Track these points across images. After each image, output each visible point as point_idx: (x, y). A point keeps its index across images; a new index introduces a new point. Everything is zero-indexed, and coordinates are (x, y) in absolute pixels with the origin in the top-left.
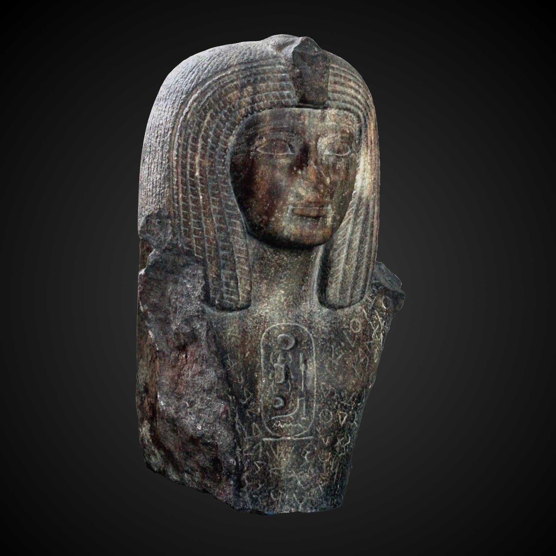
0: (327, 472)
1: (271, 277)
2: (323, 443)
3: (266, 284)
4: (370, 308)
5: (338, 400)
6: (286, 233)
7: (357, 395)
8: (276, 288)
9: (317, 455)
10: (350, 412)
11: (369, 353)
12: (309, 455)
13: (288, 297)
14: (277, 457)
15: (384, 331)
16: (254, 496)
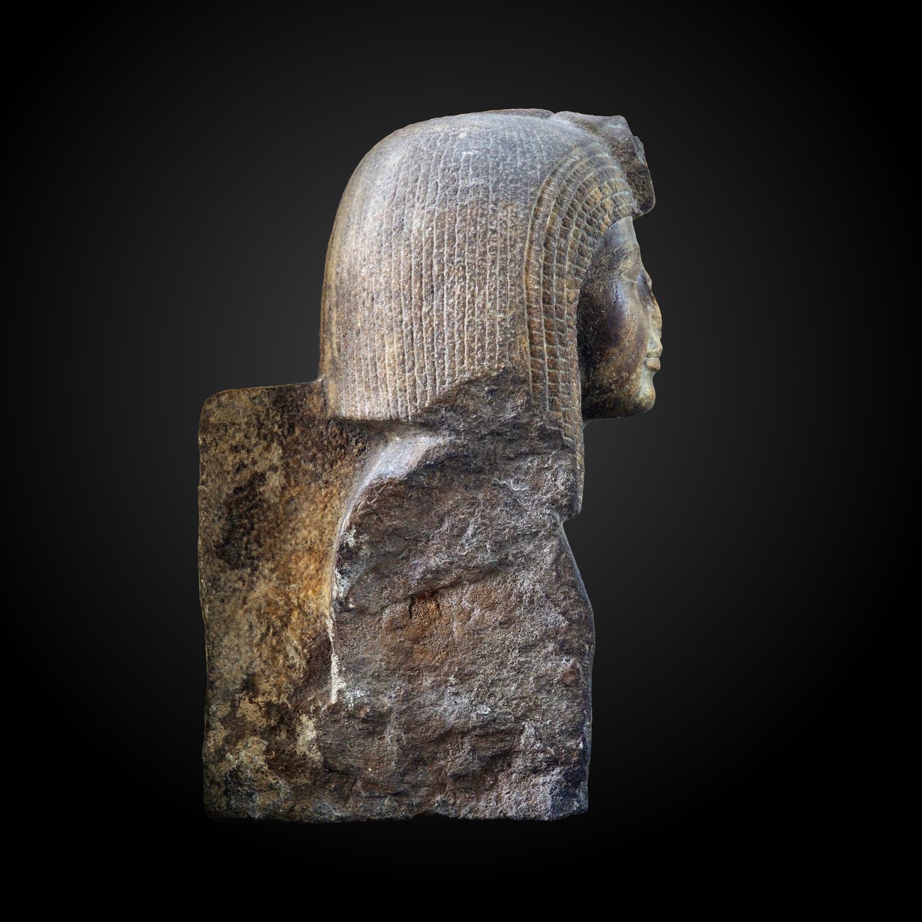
6: (641, 396)
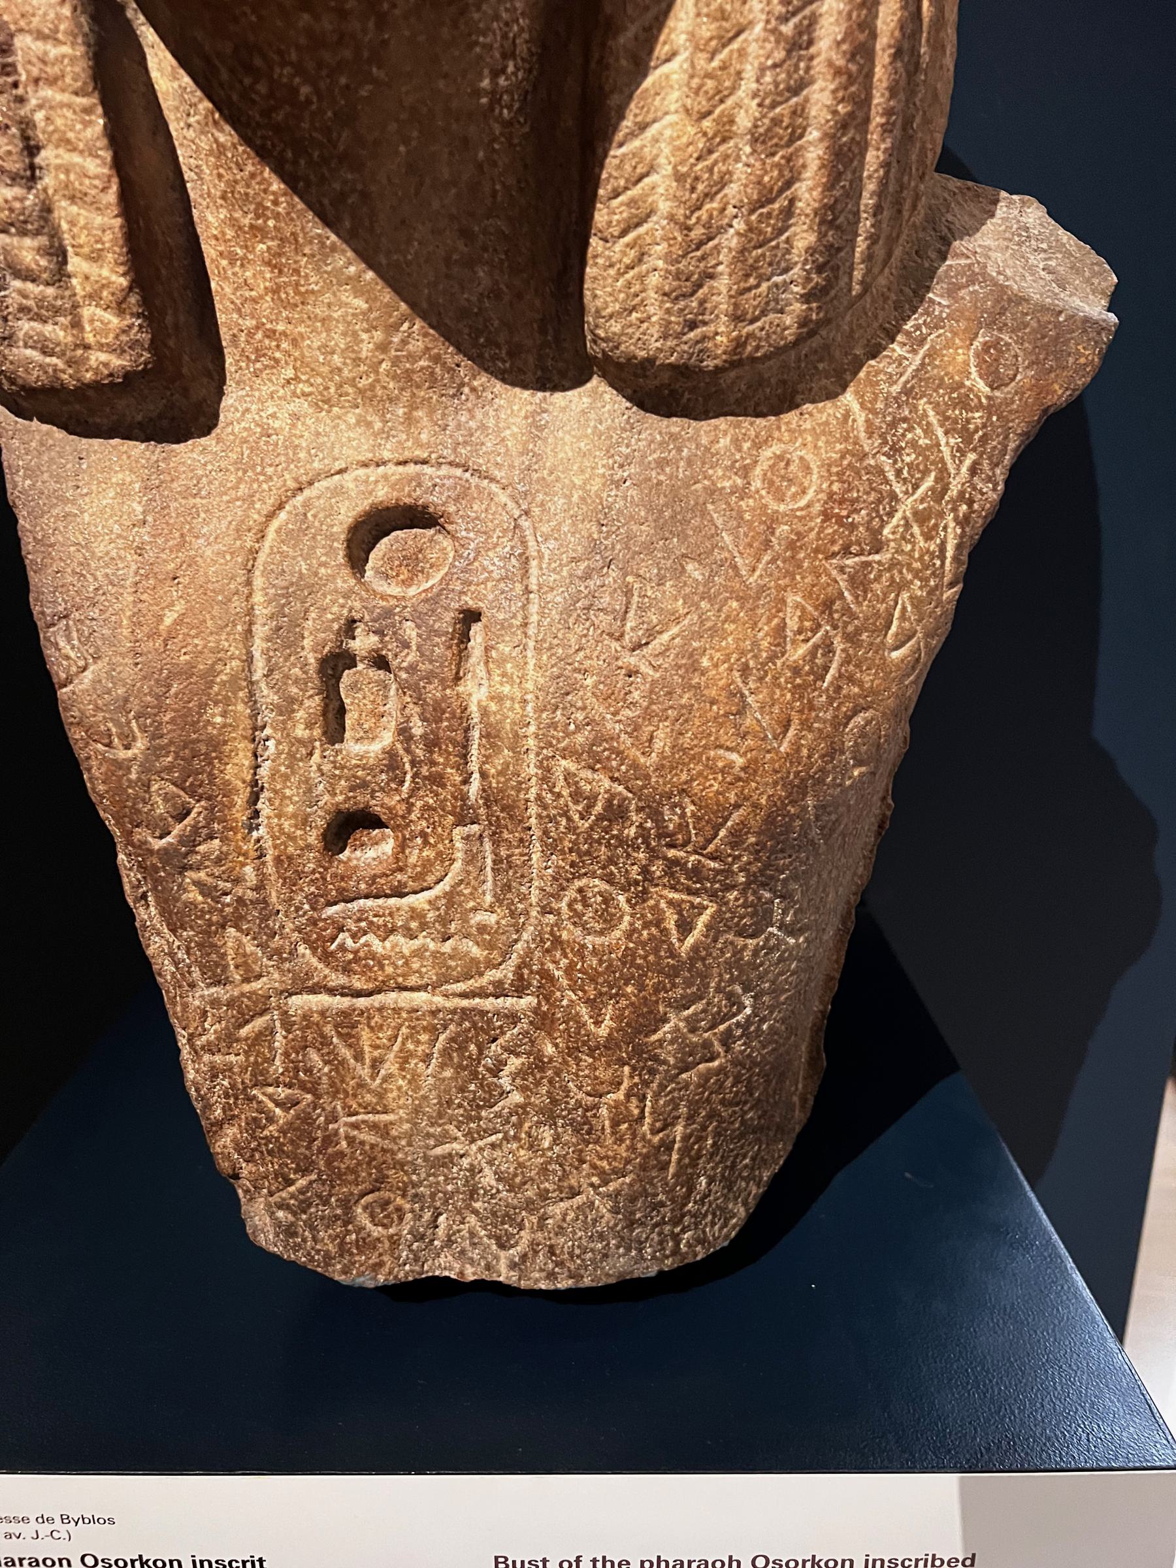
0: (621, 1140)
1: (277, 216)
2: (581, 1025)
3: (268, 264)
4: (896, 389)
5: (646, 842)
7: (755, 823)
8: (314, 282)
9: (558, 1073)
10: (732, 896)
11: (846, 610)
12: (520, 1073)
13: (396, 327)
14: (364, 1072)
15: (970, 503)
16: (280, 1214)
